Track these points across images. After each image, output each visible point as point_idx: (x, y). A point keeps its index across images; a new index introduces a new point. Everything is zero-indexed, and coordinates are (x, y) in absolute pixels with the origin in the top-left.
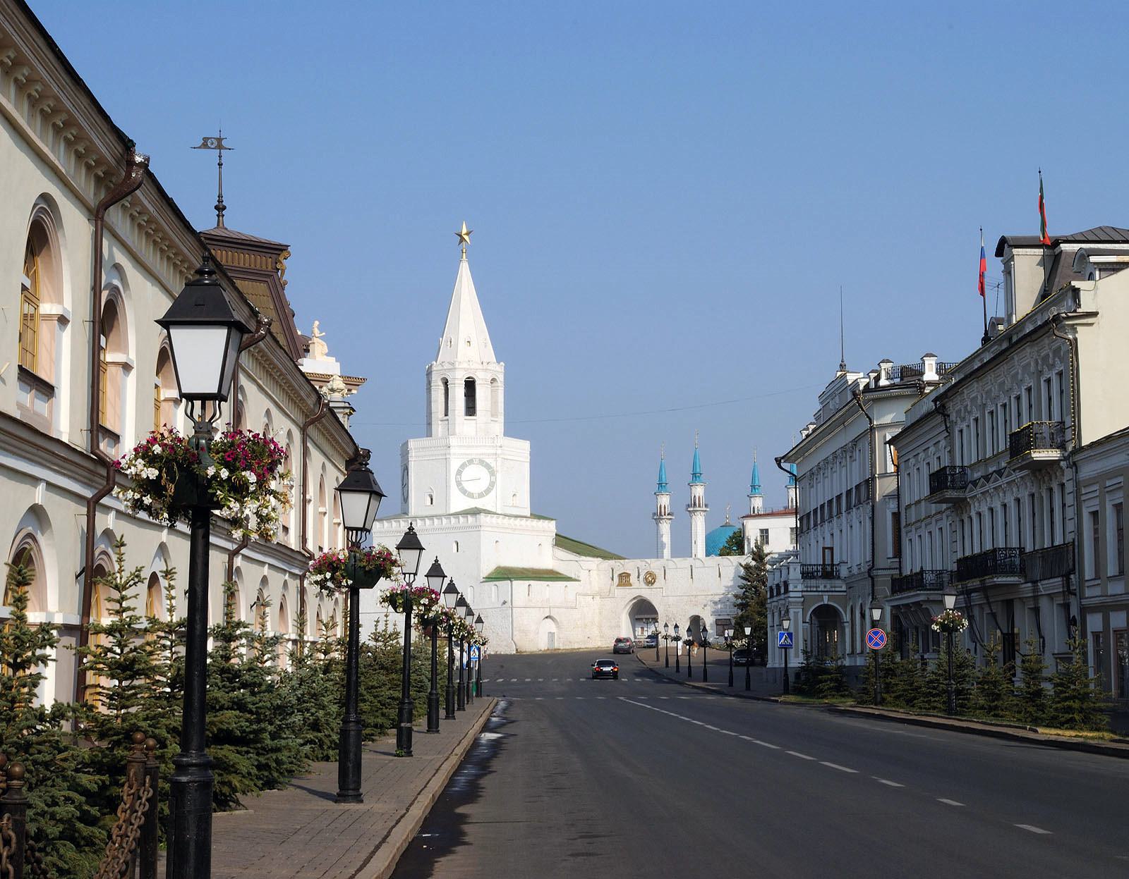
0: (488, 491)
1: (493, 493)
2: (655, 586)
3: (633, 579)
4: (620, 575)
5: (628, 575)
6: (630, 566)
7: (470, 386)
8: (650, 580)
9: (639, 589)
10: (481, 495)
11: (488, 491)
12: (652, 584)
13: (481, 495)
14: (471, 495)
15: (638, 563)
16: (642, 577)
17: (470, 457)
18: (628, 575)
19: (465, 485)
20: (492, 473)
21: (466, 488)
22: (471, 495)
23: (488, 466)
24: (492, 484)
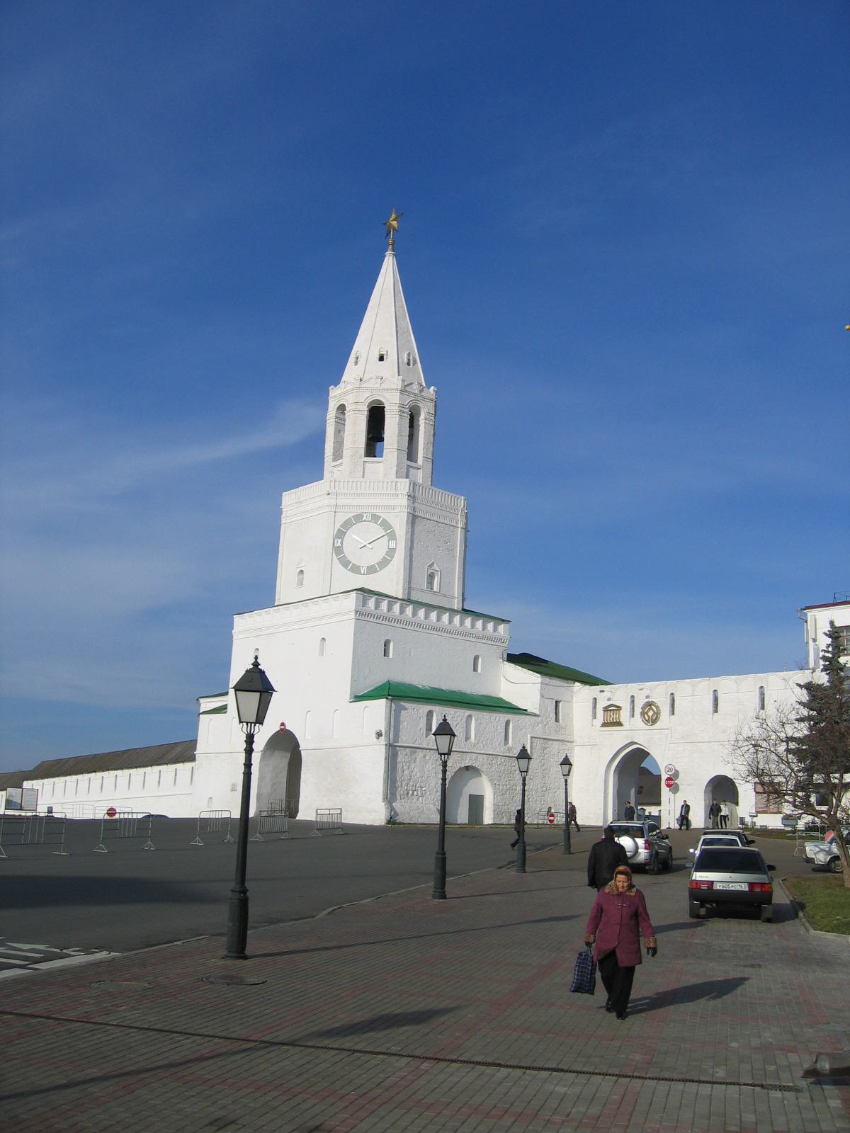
0: (384, 563)
2: (657, 725)
3: (624, 716)
4: (606, 709)
6: (618, 694)
7: (376, 415)
8: (650, 714)
9: (634, 732)
10: (372, 570)
12: (654, 721)
13: (372, 570)
14: (356, 569)
15: (633, 688)
16: (638, 711)
17: (360, 511)
18: (619, 708)
19: (348, 551)
21: (349, 558)
22: (356, 569)
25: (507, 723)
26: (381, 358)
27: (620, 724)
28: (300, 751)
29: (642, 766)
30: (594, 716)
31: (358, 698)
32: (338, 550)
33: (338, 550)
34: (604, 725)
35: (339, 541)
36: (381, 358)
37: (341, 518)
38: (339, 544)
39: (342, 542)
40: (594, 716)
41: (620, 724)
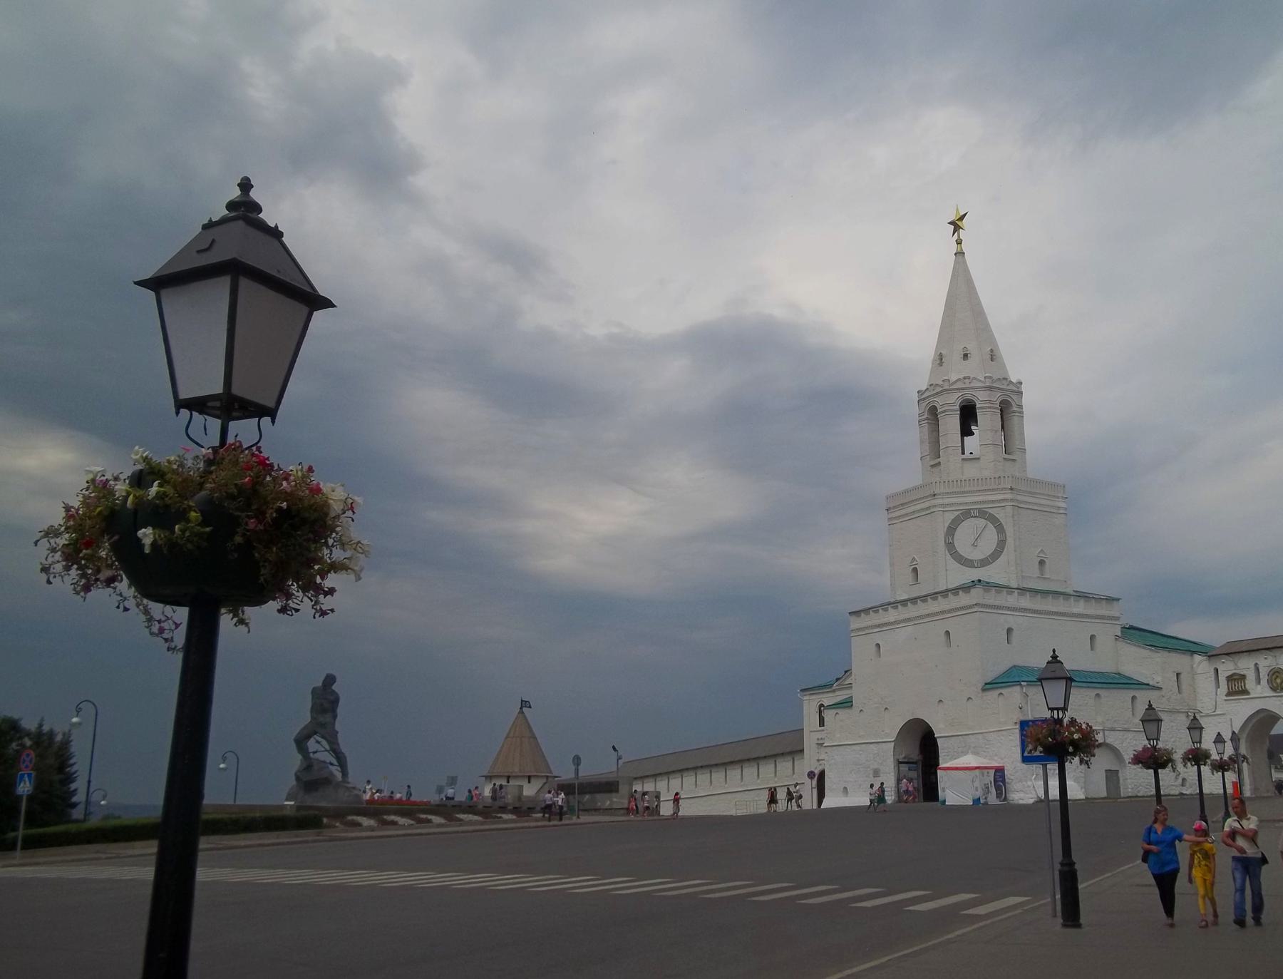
0: (996, 555)
1: (1003, 558)
3: (1250, 684)
4: (1230, 679)
5: (1243, 677)
10: (985, 563)
11: (996, 555)
13: (985, 563)
14: (969, 563)
18: (1243, 677)
20: (1000, 528)
22: (969, 563)
23: (993, 520)
24: (1002, 544)
25: (1134, 698)
26: (966, 356)
27: (1245, 692)
28: (935, 740)
29: (1273, 732)
30: (1218, 686)
31: (989, 686)
32: (950, 546)
33: (950, 546)
34: (1229, 694)
36: (966, 356)
37: (952, 516)
40: (1218, 686)
41: (1245, 692)
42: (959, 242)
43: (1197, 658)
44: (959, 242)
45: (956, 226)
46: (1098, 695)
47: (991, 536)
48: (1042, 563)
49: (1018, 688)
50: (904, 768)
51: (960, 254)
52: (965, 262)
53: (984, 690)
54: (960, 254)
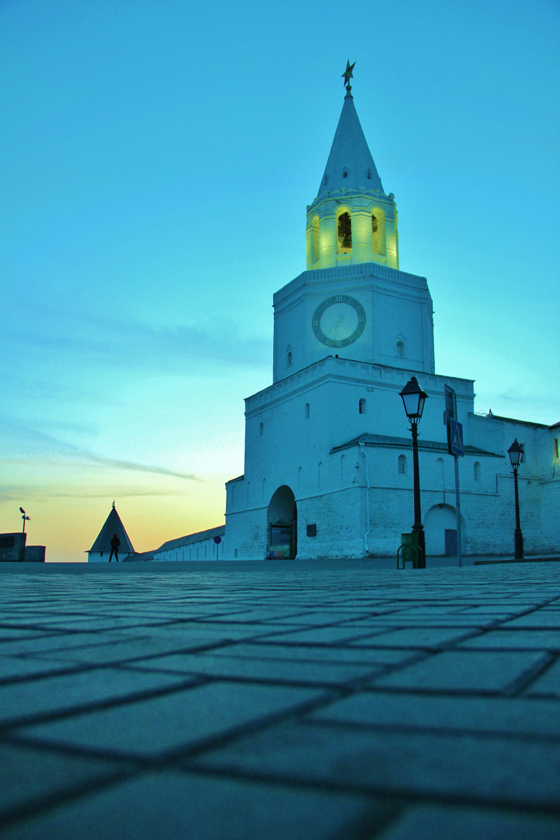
20: (361, 312)
25: (477, 464)
26: (345, 175)
35: (317, 323)
36: (345, 175)
38: (317, 324)
39: (319, 323)
42: (349, 89)
43: (540, 430)
44: (349, 89)
45: (348, 74)
46: (440, 459)
47: (353, 320)
48: (400, 344)
49: (356, 448)
50: (275, 531)
51: (349, 97)
52: (353, 103)
53: (331, 453)
54: (349, 97)
